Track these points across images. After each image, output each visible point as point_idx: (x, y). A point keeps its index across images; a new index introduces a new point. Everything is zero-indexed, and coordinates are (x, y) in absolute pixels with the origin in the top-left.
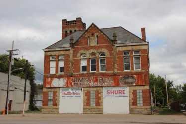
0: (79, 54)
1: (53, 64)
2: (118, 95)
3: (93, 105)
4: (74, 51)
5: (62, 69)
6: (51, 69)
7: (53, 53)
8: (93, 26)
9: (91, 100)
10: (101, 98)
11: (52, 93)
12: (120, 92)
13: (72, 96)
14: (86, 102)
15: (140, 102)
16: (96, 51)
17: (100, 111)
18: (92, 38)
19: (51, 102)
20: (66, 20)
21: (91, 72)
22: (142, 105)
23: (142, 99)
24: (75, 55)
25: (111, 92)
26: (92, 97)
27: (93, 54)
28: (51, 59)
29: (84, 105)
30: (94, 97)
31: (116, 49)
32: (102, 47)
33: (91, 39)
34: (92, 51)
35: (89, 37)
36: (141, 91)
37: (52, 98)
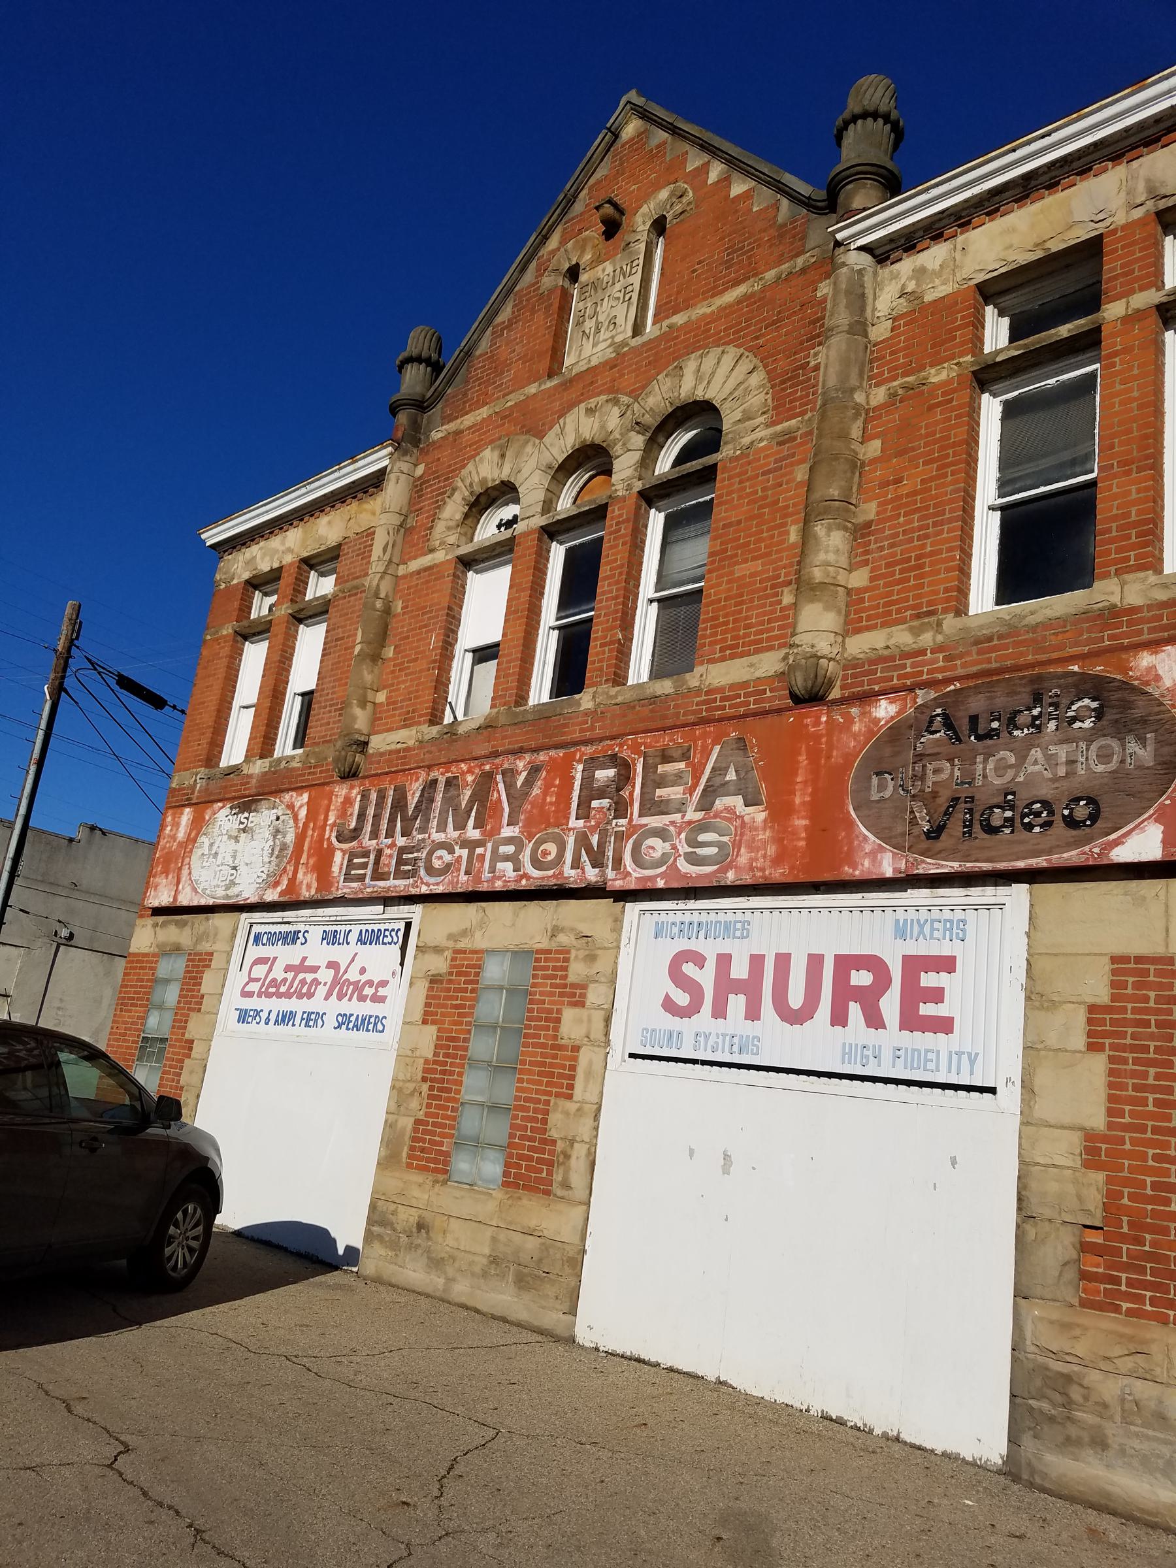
2: (819, 1042)
10: (585, 1057)
12: (853, 987)
13: (310, 1019)
25: (725, 985)
27: (592, 457)
31: (858, 299)
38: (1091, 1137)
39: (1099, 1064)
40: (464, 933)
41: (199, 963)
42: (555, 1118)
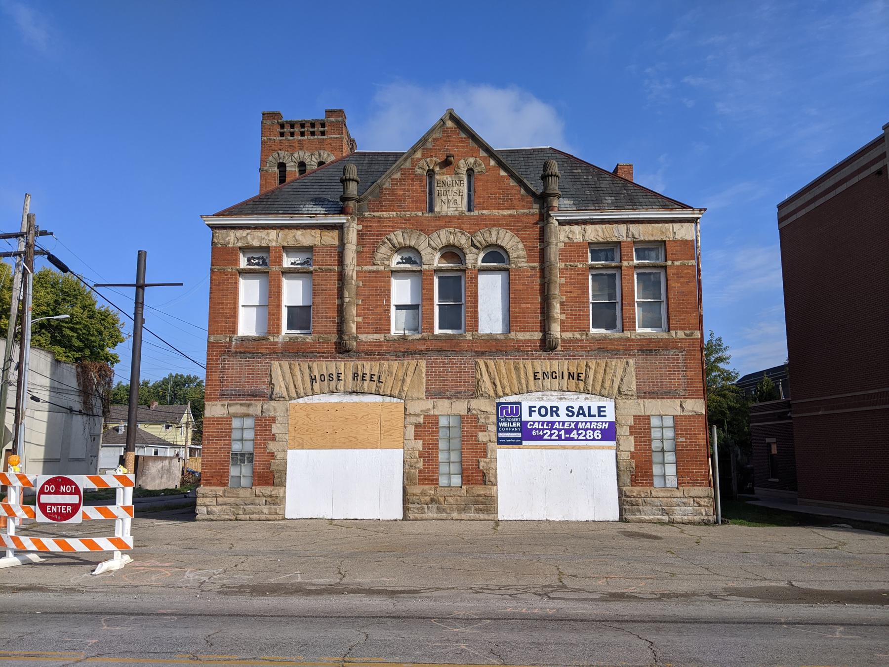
0: (384, 250)
1: (249, 291)
3: (450, 478)
4: (361, 235)
5: (300, 317)
6: (242, 313)
7: (255, 239)
8: (450, 124)
9: (442, 457)
11: (249, 422)
14: (421, 465)
15: (667, 470)
16: (463, 241)
17: (488, 504)
18: (448, 179)
19: (246, 469)
20: (277, 115)
21: (437, 331)
22: (672, 482)
23: (670, 457)
24: (366, 254)
26: (442, 445)
28: (243, 263)
29: (408, 480)
30: (456, 444)
32: (496, 223)
33: (444, 183)
34: (444, 237)
35: (431, 173)
36: (669, 422)
37: (249, 447)
38: (631, 453)
39: (632, 438)
40: (429, 410)
42: (482, 464)
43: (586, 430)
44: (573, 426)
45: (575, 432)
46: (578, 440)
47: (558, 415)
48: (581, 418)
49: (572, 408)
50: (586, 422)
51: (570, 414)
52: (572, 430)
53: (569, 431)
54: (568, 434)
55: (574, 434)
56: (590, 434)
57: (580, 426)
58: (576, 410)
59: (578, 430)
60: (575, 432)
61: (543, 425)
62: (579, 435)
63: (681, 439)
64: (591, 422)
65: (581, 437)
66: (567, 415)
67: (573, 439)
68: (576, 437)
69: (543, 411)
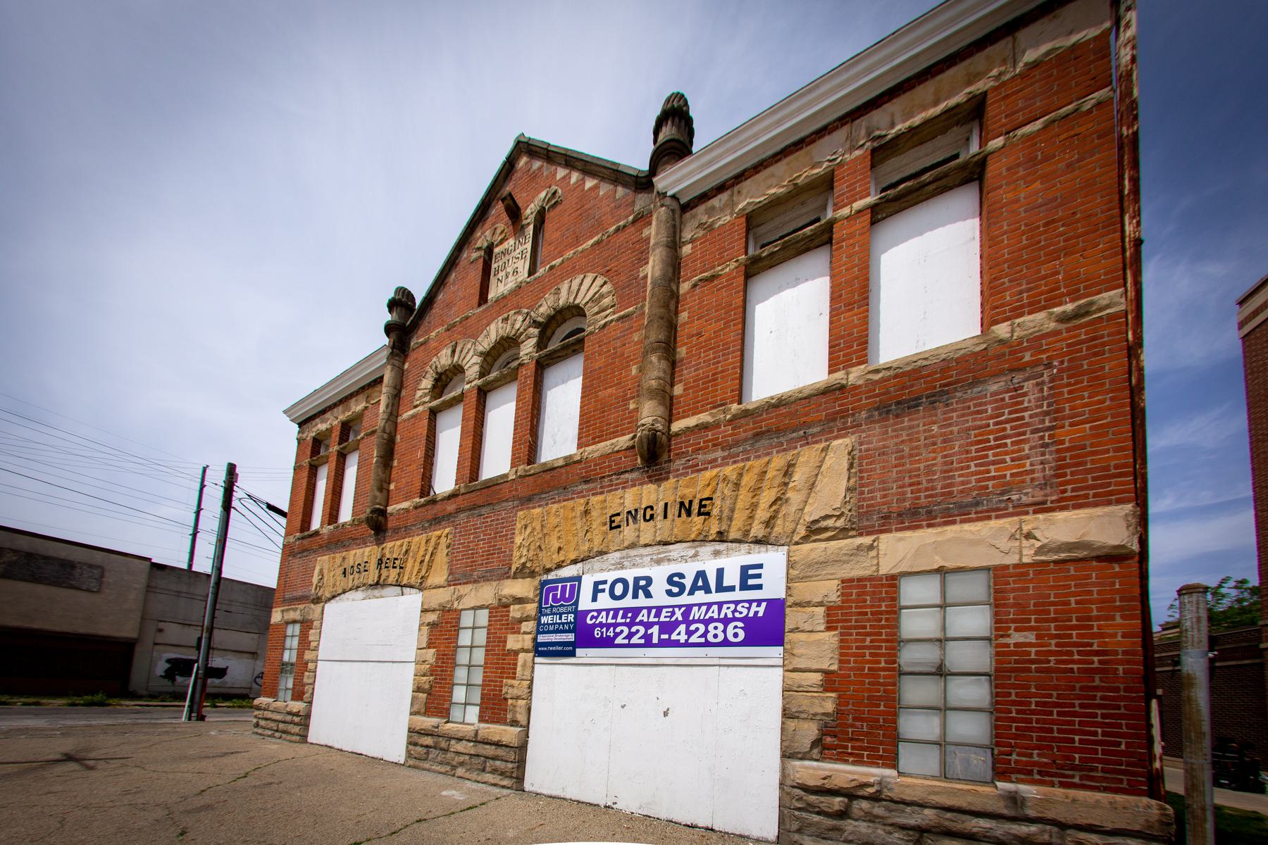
41: (306, 625)
43: (706, 622)
44: (678, 615)
45: (682, 628)
46: (687, 644)
47: (648, 595)
48: (700, 597)
49: (681, 576)
50: (709, 605)
51: (675, 590)
52: (677, 623)
53: (668, 627)
54: (665, 632)
55: (680, 634)
56: (716, 631)
57: (695, 614)
58: (688, 582)
59: (688, 623)
60: (682, 628)
61: (615, 617)
62: (690, 633)
63: (1016, 638)
64: (720, 605)
65: (694, 639)
66: (669, 593)
67: (677, 644)
68: (683, 638)
69: (619, 589)
